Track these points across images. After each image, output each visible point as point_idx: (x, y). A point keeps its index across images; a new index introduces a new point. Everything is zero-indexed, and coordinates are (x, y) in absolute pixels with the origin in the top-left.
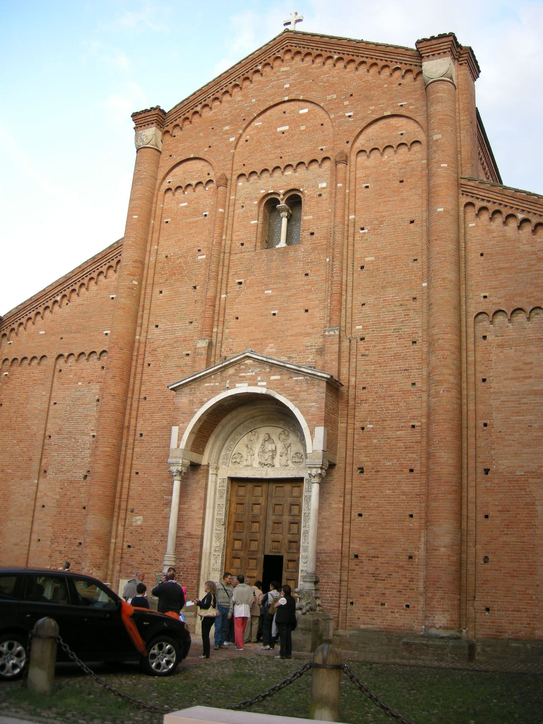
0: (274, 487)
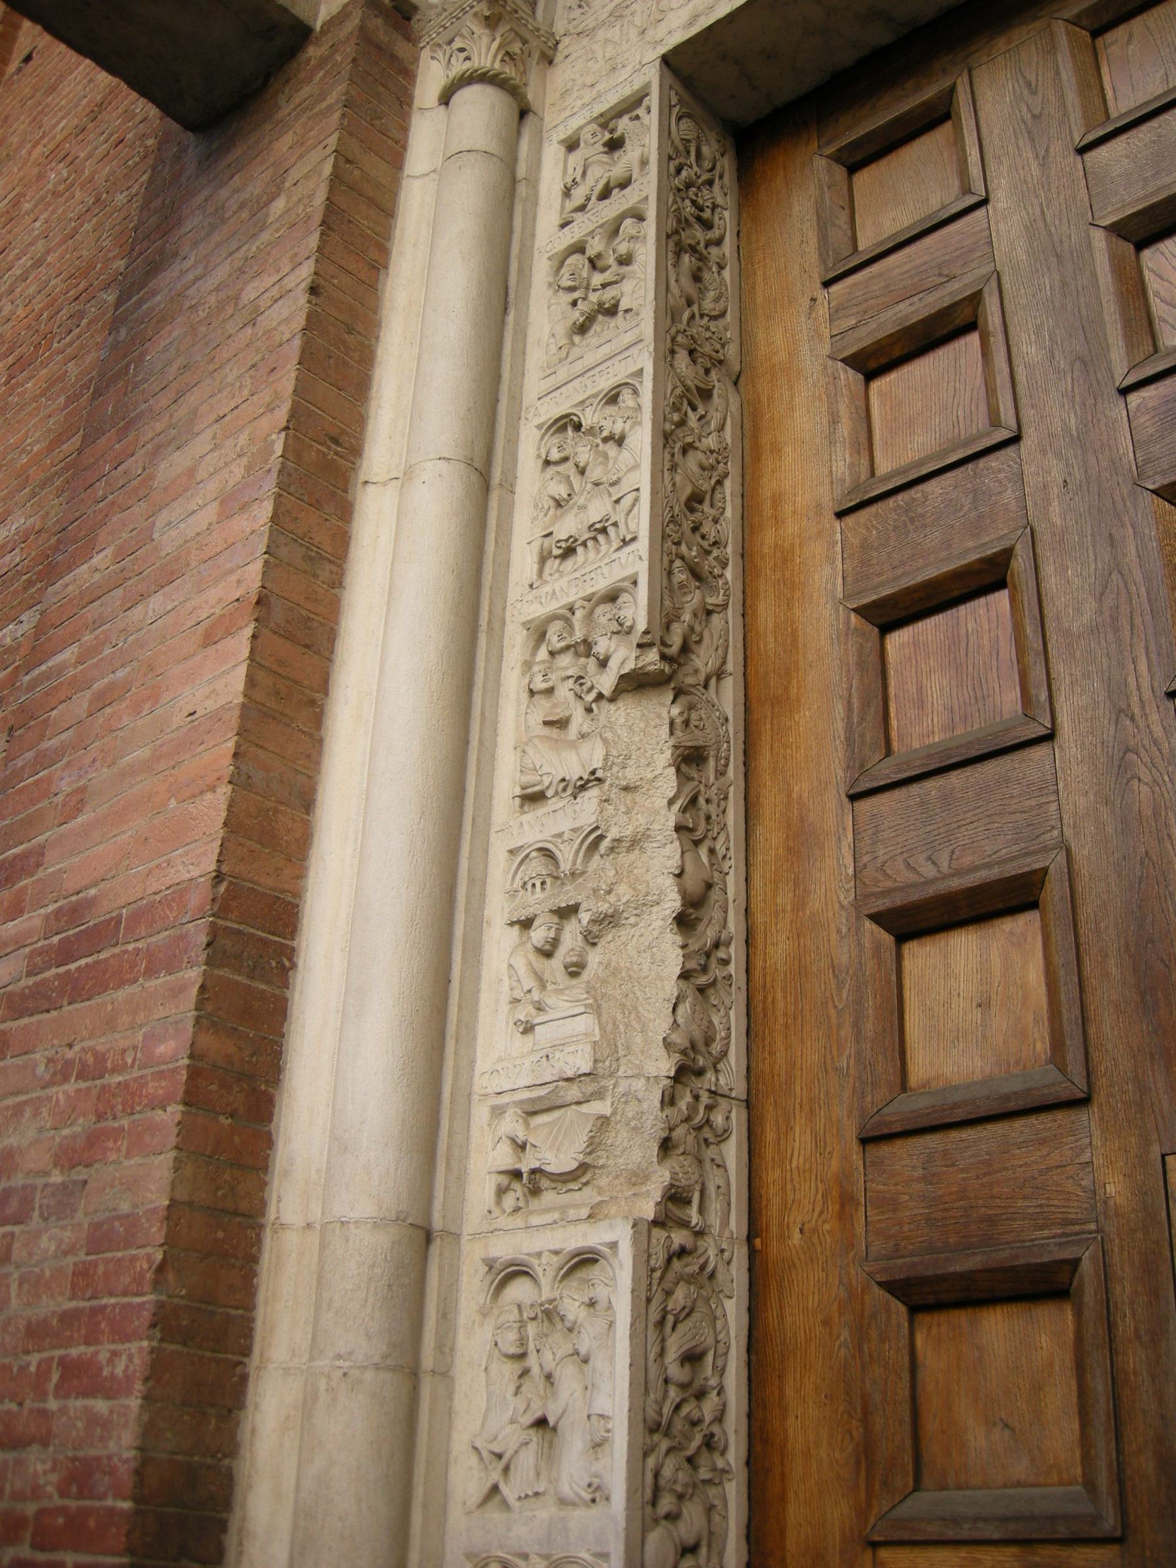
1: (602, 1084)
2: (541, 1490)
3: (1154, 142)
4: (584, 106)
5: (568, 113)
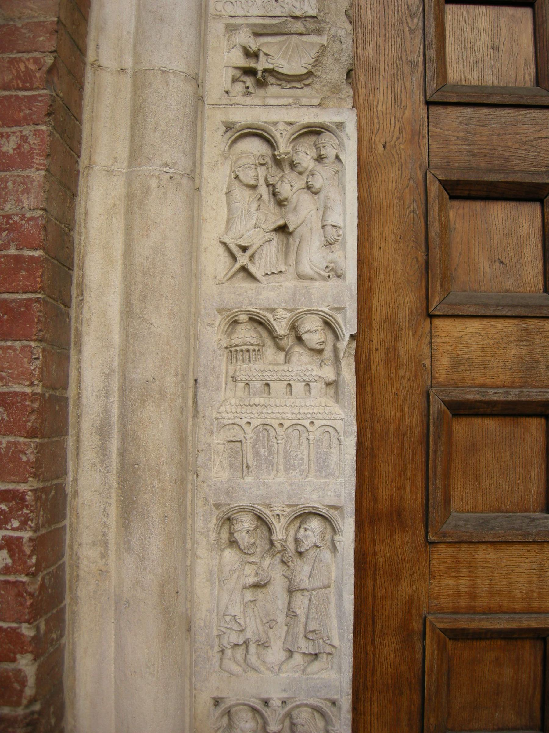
1: (323, 25)
2: (283, 270)
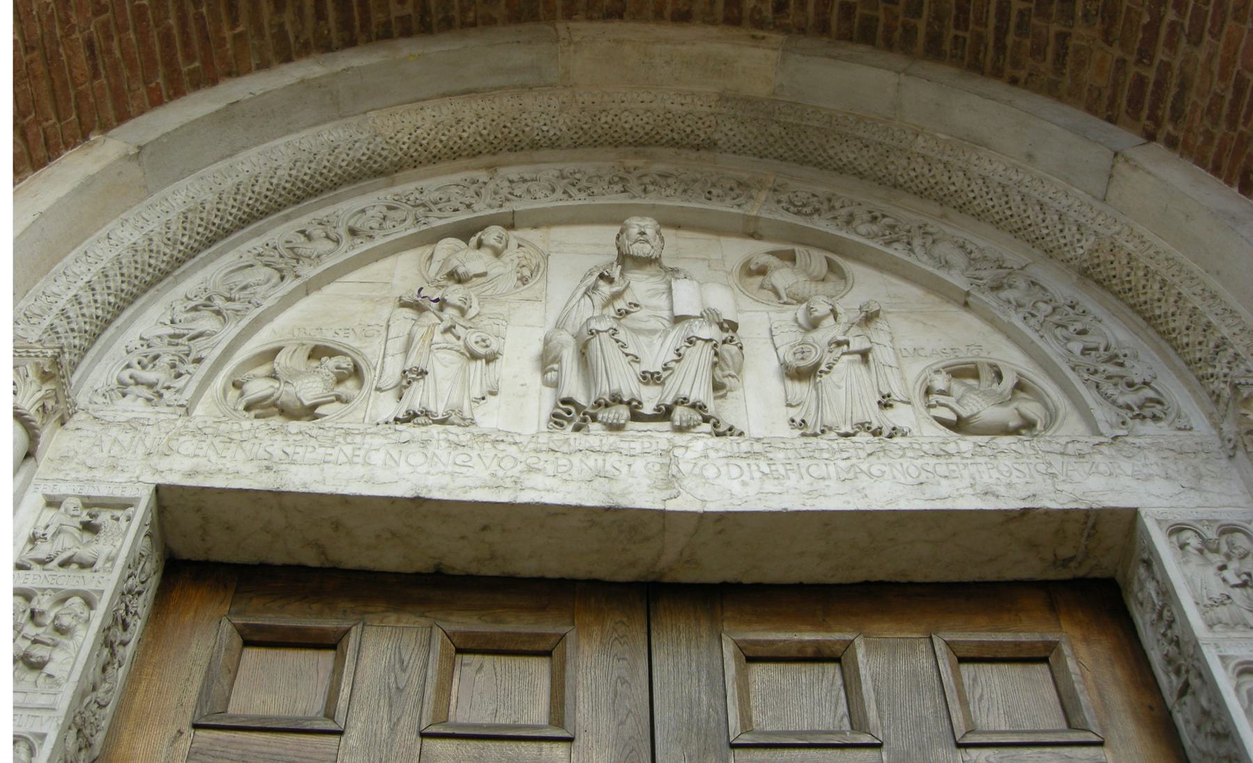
0: (729, 650)
3: (475, 758)
4: (77, 480)
5: (61, 476)
